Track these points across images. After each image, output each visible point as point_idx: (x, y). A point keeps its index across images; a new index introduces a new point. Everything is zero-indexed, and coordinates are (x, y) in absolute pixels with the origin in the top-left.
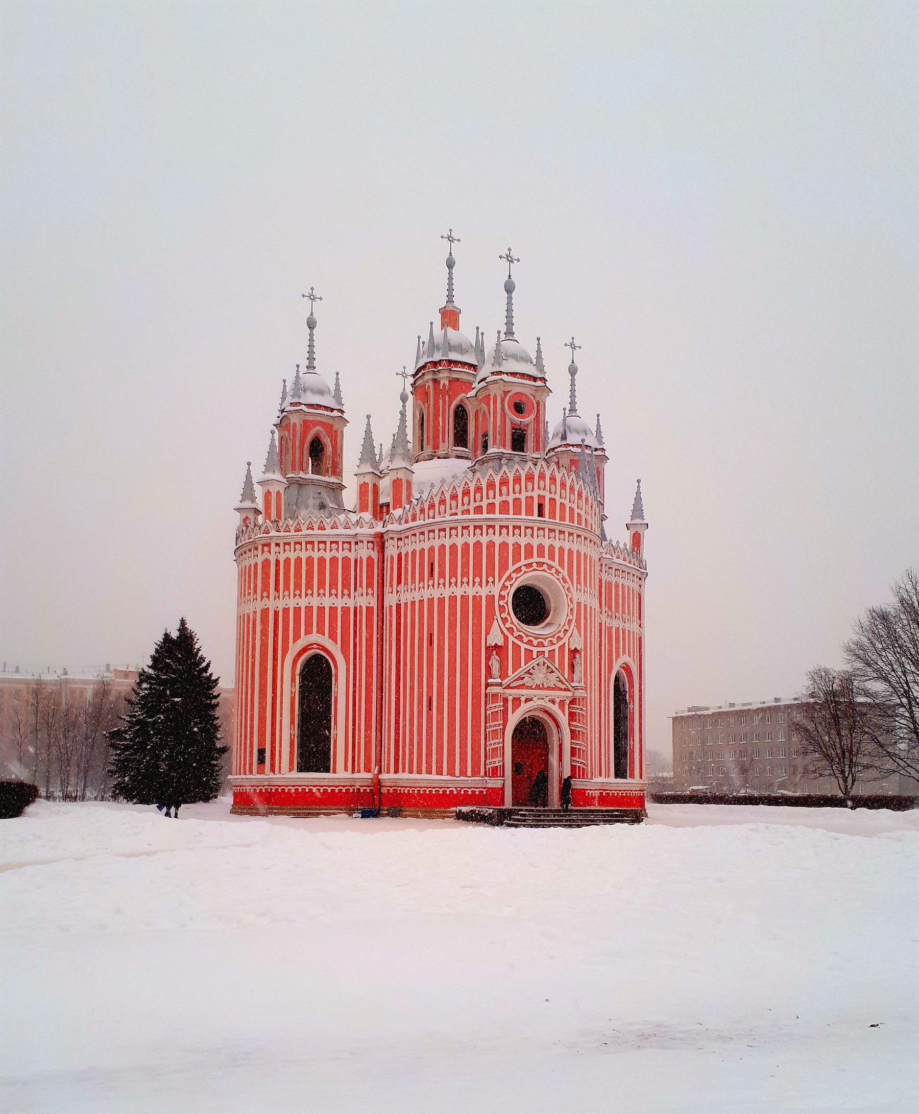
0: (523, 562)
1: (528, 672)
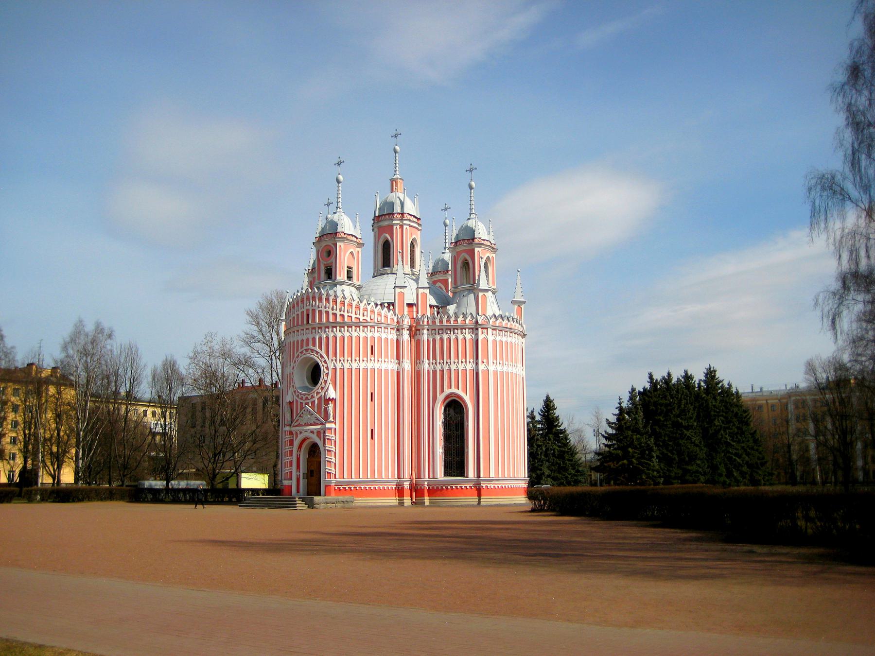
0: (300, 350)
1: (300, 416)
